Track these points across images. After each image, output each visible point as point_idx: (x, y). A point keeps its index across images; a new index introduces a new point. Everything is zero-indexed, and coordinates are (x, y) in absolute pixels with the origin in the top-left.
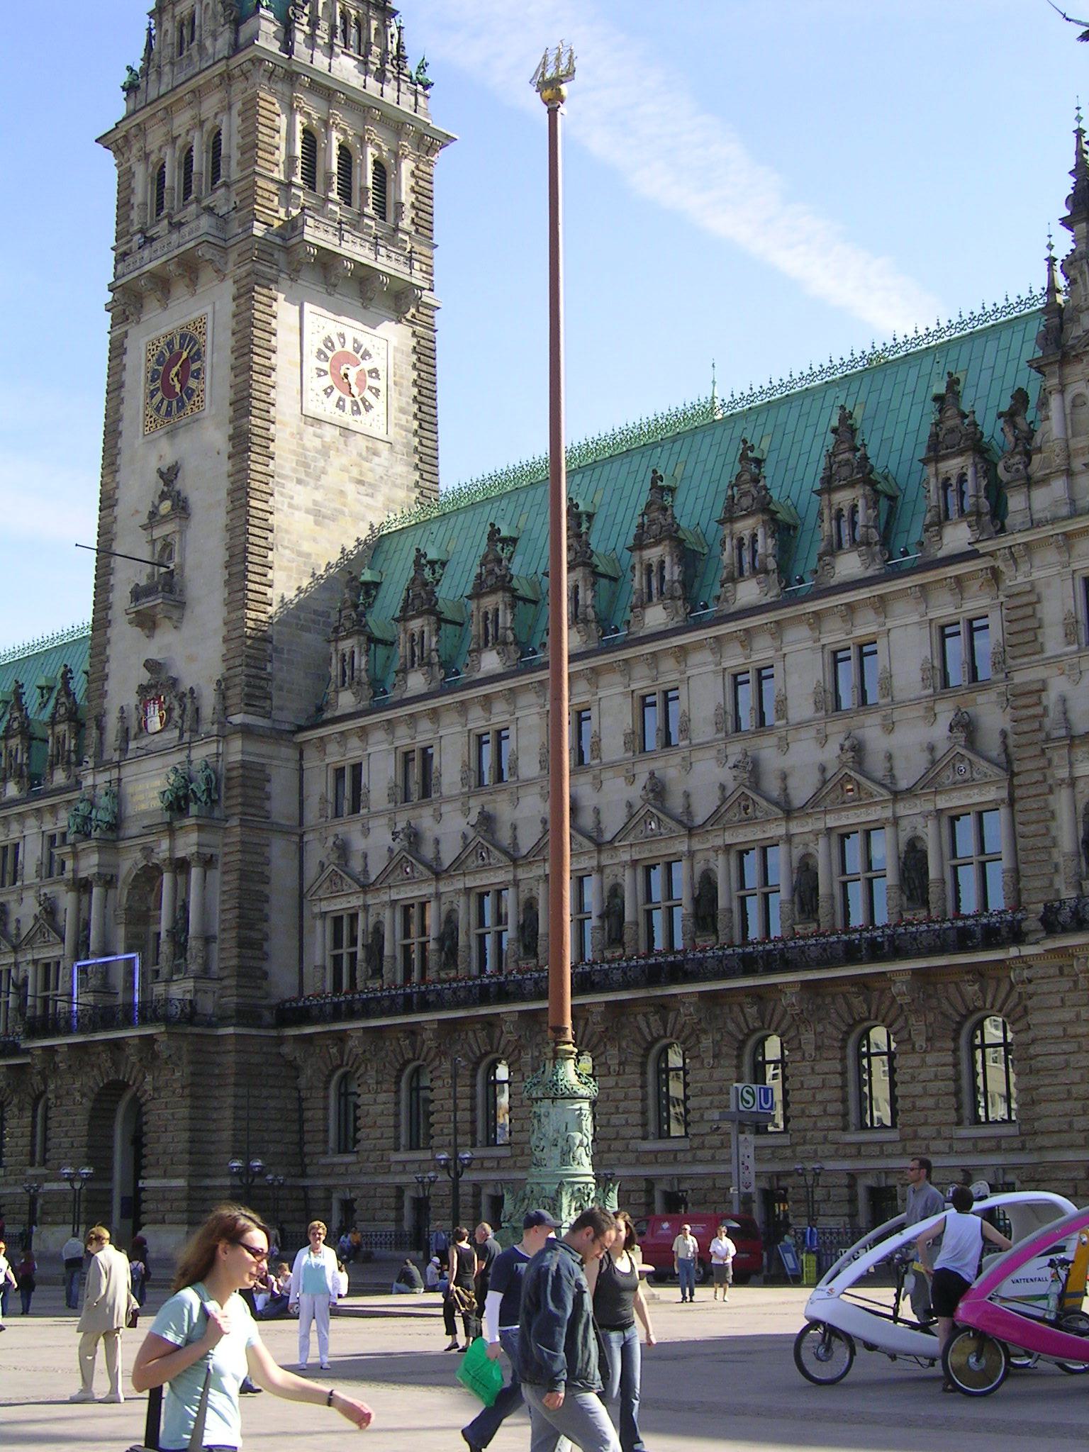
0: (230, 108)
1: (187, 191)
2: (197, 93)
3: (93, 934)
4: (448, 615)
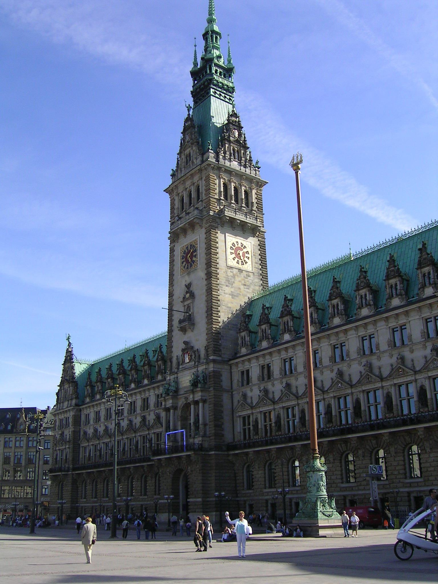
0: (202, 178)
1: (190, 203)
2: (192, 175)
3: (171, 424)
4: (273, 323)
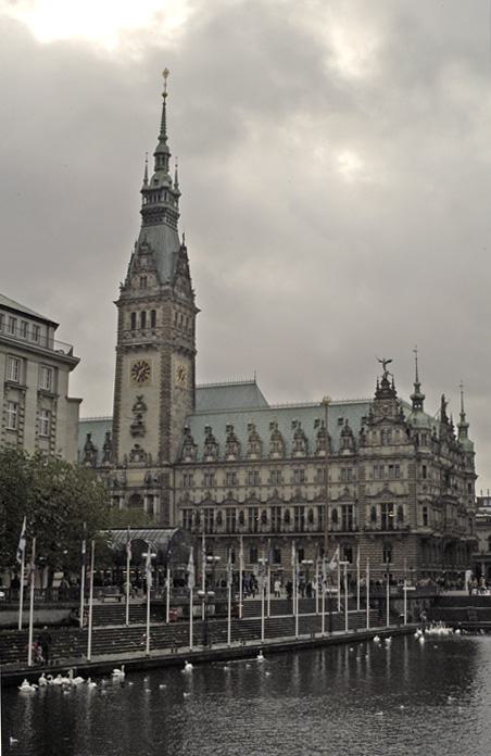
2: (150, 301)
